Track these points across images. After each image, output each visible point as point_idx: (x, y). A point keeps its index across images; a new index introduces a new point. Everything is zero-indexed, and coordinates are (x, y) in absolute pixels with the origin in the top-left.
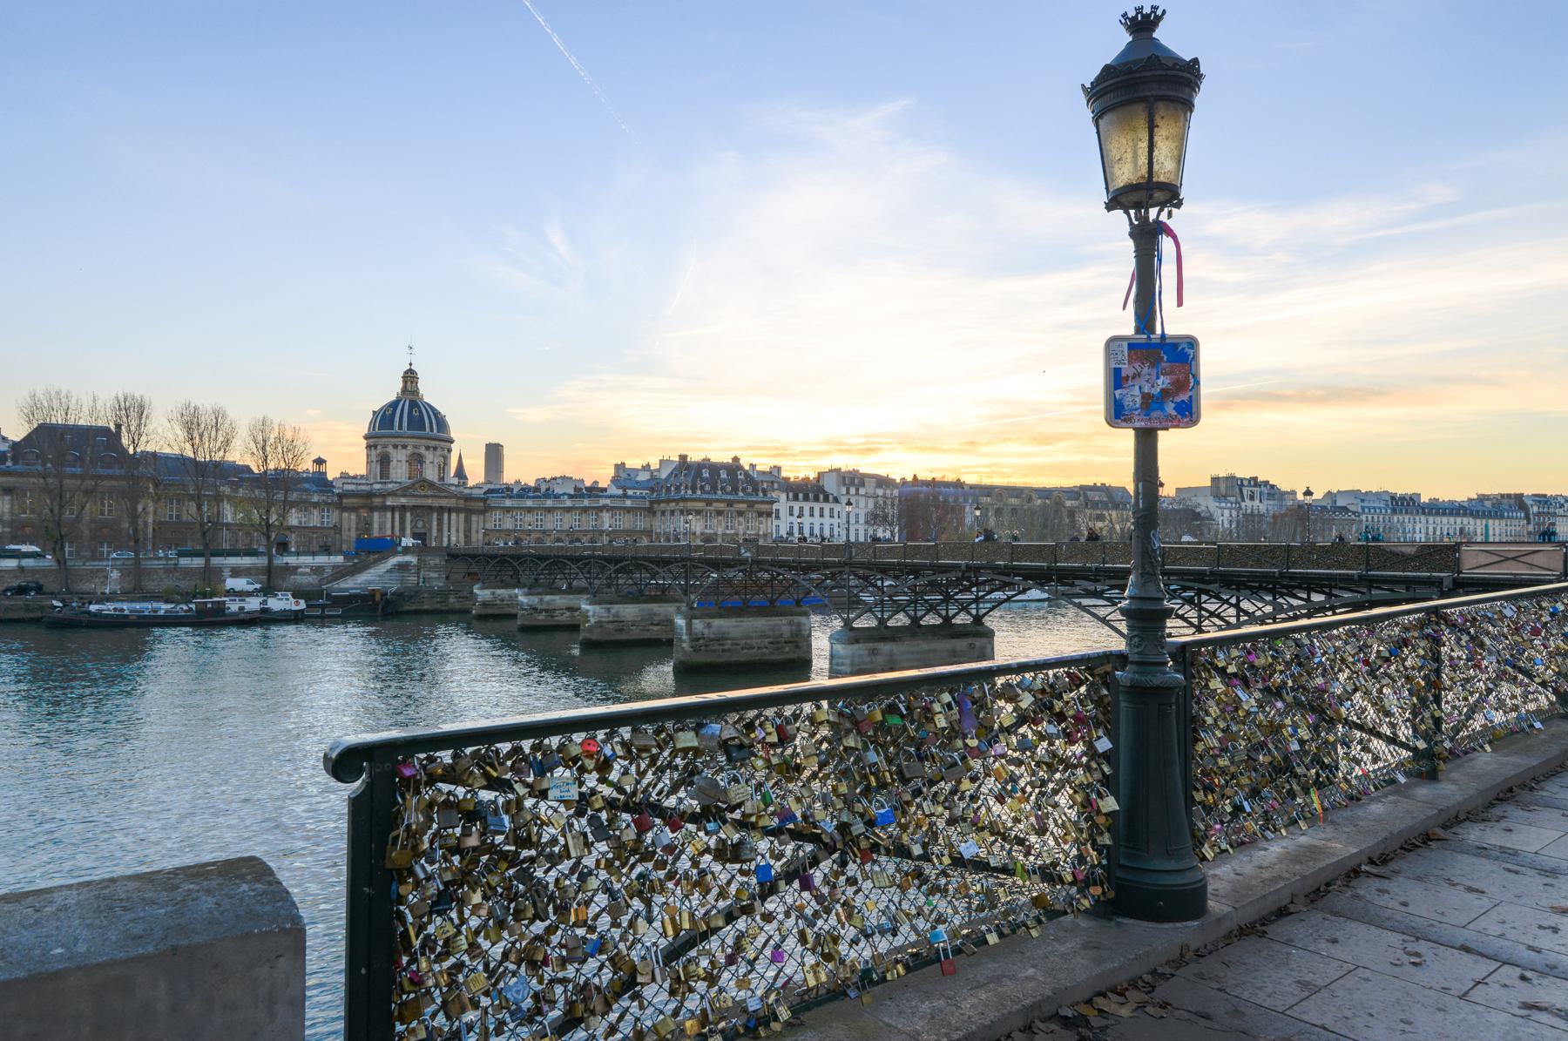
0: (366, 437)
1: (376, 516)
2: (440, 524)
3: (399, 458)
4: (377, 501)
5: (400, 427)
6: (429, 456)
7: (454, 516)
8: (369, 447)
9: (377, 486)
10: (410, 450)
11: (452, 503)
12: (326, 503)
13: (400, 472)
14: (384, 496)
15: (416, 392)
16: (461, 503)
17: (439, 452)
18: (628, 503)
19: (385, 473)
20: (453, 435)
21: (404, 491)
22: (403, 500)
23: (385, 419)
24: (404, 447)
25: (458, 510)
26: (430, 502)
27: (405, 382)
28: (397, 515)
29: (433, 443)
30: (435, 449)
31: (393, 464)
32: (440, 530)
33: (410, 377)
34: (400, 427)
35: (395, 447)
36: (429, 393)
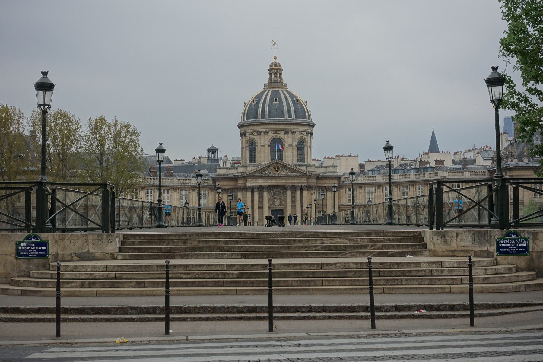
0: (240, 126)
2: (294, 201)
3: (263, 142)
5: (263, 116)
7: (305, 193)
8: (241, 135)
9: (241, 170)
10: (271, 136)
11: (303, 182)
14: (245, 178)
15: (280, 82)
16: (313, 182)
17: (298, 136)
18: (467, 175)
19: (252, 159)
20: (314, 119)
22: (261, 182)
23: (252, 111)
24: (266, 133)
25: (309, 188)
28: (256, 194)
29: (292, 128)
30: (293, 133)
31: (258, 149)
32: (294, 207)
34: (263, 116)
35: (259, 133)
36: (292, 82)
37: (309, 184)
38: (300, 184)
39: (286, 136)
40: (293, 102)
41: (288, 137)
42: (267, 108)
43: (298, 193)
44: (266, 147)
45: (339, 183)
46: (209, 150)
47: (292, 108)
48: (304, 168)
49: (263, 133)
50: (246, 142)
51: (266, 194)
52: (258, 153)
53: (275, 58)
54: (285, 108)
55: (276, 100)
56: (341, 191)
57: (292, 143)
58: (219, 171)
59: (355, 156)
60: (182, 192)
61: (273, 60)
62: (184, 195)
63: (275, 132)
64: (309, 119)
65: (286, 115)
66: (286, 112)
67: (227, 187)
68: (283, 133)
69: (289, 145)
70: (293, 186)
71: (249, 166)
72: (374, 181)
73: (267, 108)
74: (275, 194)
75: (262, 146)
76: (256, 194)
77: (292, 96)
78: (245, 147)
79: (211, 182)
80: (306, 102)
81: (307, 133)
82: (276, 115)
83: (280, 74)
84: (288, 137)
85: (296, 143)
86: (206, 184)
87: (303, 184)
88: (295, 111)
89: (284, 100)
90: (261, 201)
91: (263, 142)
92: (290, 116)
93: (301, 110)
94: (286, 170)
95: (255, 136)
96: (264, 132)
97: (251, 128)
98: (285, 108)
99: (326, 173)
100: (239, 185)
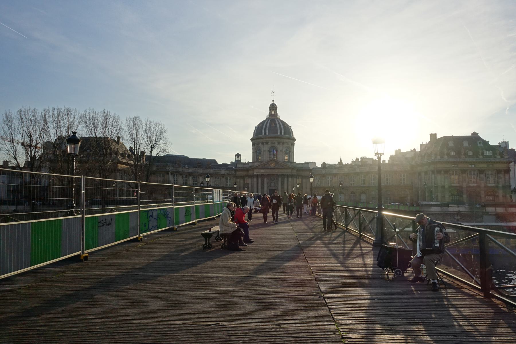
0: (252, 140)
4: (250, 172)
6: (280, 148)
7: (290, 179)
9: (250, 165)
10: (270, 145)
12: (229, 175)
13: (265, 157)
15: (276, 114)
20: (295, 136)
21: (264, 165)
22: (262, 172)
23: (259, 130)
24: (267, 143)
26: (276, 172)
27: (270, 110)
30: (283, 143)
33: (273, 107)
34: (265, 134)
35: (263, 143)
36: (282, 115)
40: (283, 125)
42: (267, 129)
43: (286, 179)
46: (236, 155)
47: (283, 129)
48: (289, 164)
50: (255, 149)
51: (266, 180)
53: (273, 101)
54: (278, 128)
58: (239, 166)
60: (216, 178)
62: (217, 180)
63: (272, 143)
65: (279, 133)
66: (279, 131)
70: (283, 175)
71: (256, 162)
73: (267, 129)
75: (264, 151)
77: (283, 122)
79: (233, 172)
82: (273, 134)
83: (276, 110)
86: (230, 173)
88: (284, 130)
89: (278, 124)
90: (263, 184)
91: (265, 148)
92: (281, 133)
93: (287, 130)
95: (260, 145)
97: (258, 140)
98: (278, 128)
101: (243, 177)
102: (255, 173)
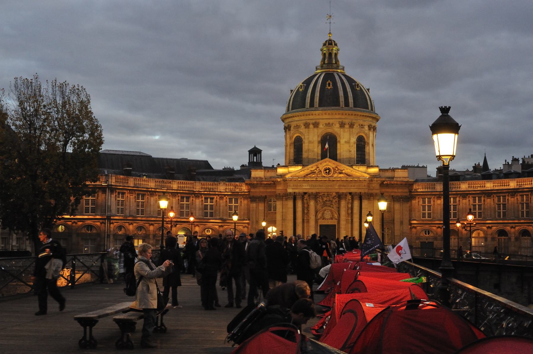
1: (279, 204)
7: (365, 203)
10: (322, 130)
24: (316, 125)
30: (351, 126)
34: (312, 104)
35: (307, 125)
37: (371, 192)
38: (358, 191)
39: (342, 130)
41: (344, 132)
42: (317, 94)
44: (316, 144)
45: (410, 192)
46: (251, 152)
49: (311, 126)
52: (306, 152)
54: (341, 93)
55: (329, 84)
56: (414, 202)
57: (350, 139)
59: (423, 167)
61: (328, 39)
64: (372, 110)
66: (342, 99)
67: (263, 195)
68: (338, 125)
69: (345, 142)
72: (458, 190)
73: (317, 94)
74: (324, 204)
75: (310, 142)
76: (299, 204)
78: (289, 144)
80: (368, 90)
81: (370, 127)
84: (344, 132)
85: (354, 140)
87: (362, 191)
92: (347, 104)
94: (340, 173)
95: (302, 129)
96: (313, 124)
98: (341, 93)
99: (393, 178)
100: (278, 192)
101: (264, 199)
102: (290, 190)
